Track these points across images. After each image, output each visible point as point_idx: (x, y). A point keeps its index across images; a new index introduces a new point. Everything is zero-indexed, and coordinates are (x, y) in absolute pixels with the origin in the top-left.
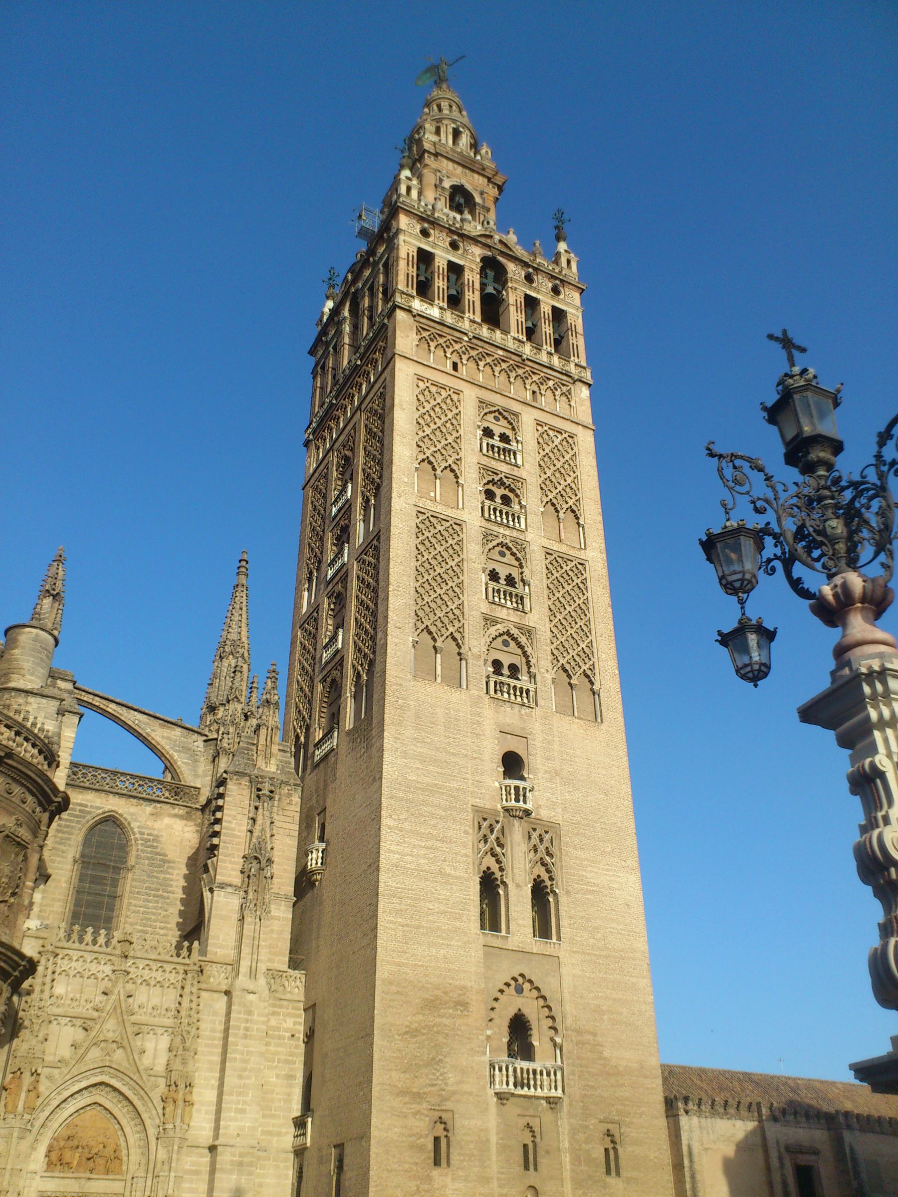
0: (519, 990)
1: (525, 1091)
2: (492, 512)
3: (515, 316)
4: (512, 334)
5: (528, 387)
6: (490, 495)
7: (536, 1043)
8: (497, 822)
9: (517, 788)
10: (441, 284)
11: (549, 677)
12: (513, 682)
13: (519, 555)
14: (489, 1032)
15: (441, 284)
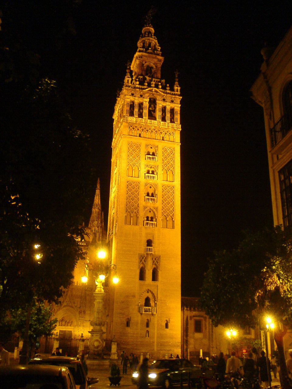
0: (148, 292)
1: (147, 313)
2: (148, 177)
3: (158, 114)
4: (157, 120)
5: (161, 136)
6: (148, 172)
7: (151, 303)
8: (145, 256)
9: (149, 249)
10: (136, 110)
11: (161, 219)
12: (152, 222)
13: (155, 187)
14: (140, 301)
15: (136, 110)
